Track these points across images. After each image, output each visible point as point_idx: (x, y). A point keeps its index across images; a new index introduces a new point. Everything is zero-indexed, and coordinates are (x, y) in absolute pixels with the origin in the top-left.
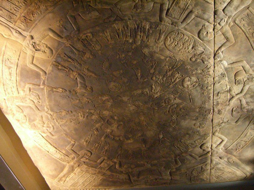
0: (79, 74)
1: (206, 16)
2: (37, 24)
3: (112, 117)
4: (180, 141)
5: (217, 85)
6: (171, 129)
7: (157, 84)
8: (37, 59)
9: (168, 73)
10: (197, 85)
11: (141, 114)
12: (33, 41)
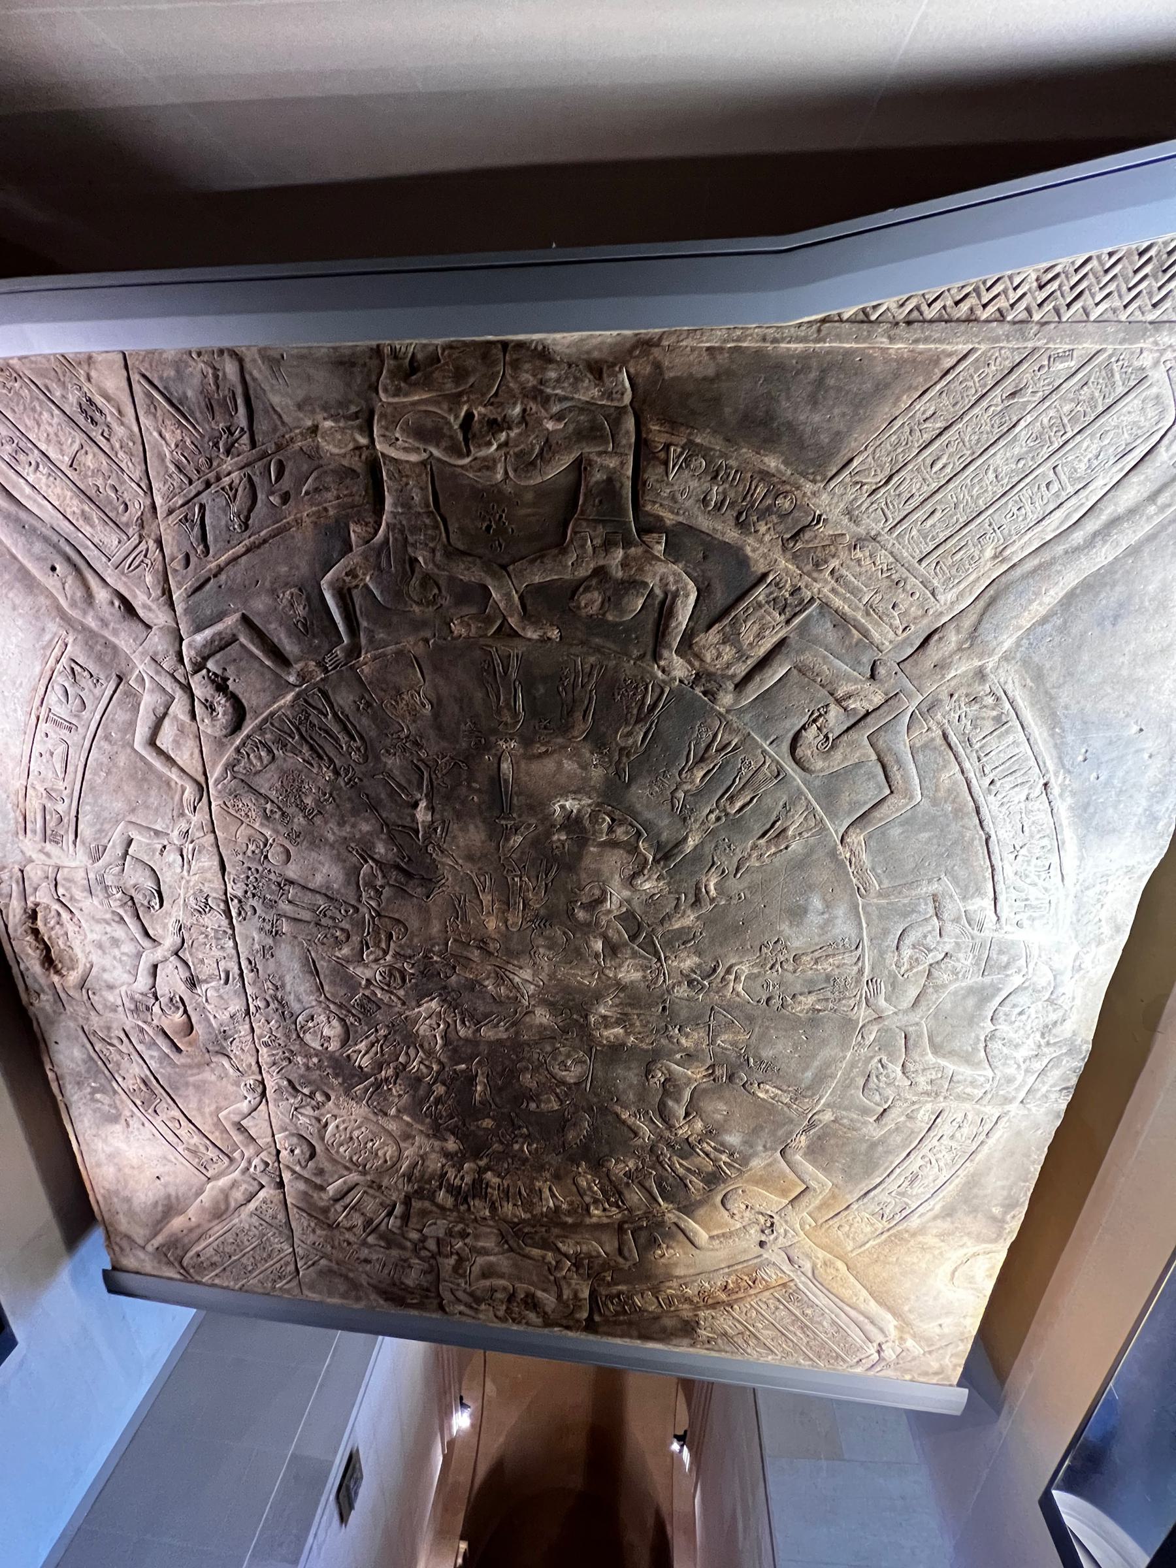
0: (670, 1127)
1: (301, 1186)
2: (729, 1267)
3: (612, 949)
4: (336, 773)
5: (236, 1006)
6: (380, 849)
7: (426, 1046)
8: (784, 1193)
9: (390, 1072)
10: (300, 1018)
11: (492, 946)
12: (763, 1238)
